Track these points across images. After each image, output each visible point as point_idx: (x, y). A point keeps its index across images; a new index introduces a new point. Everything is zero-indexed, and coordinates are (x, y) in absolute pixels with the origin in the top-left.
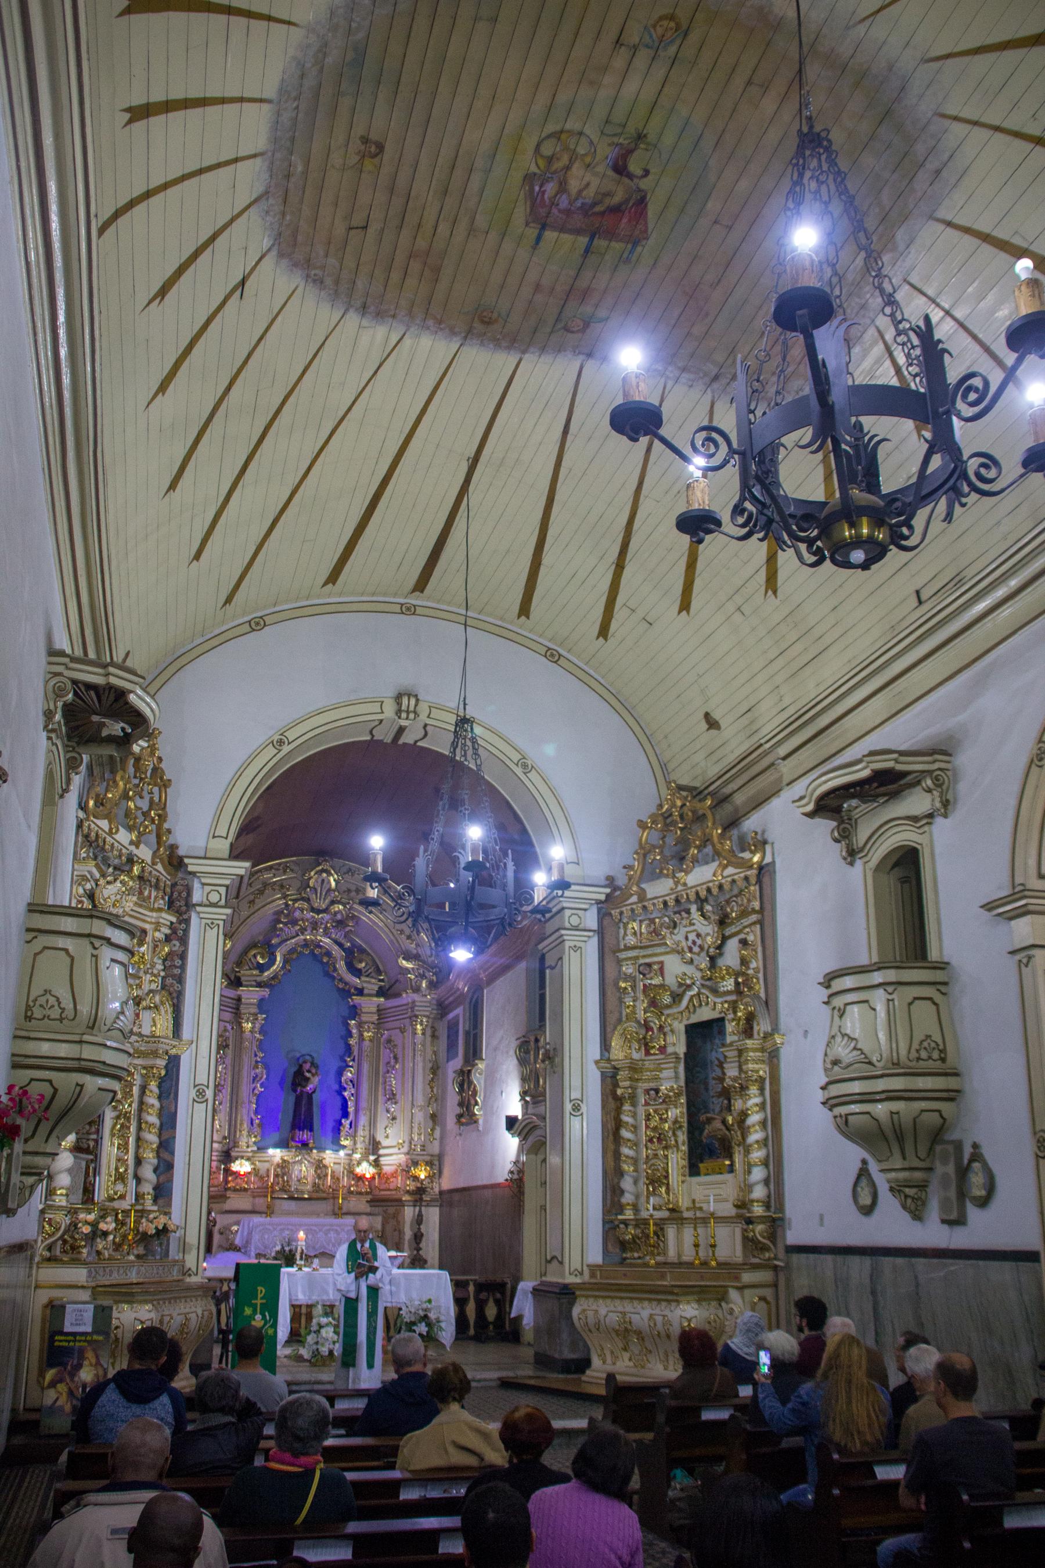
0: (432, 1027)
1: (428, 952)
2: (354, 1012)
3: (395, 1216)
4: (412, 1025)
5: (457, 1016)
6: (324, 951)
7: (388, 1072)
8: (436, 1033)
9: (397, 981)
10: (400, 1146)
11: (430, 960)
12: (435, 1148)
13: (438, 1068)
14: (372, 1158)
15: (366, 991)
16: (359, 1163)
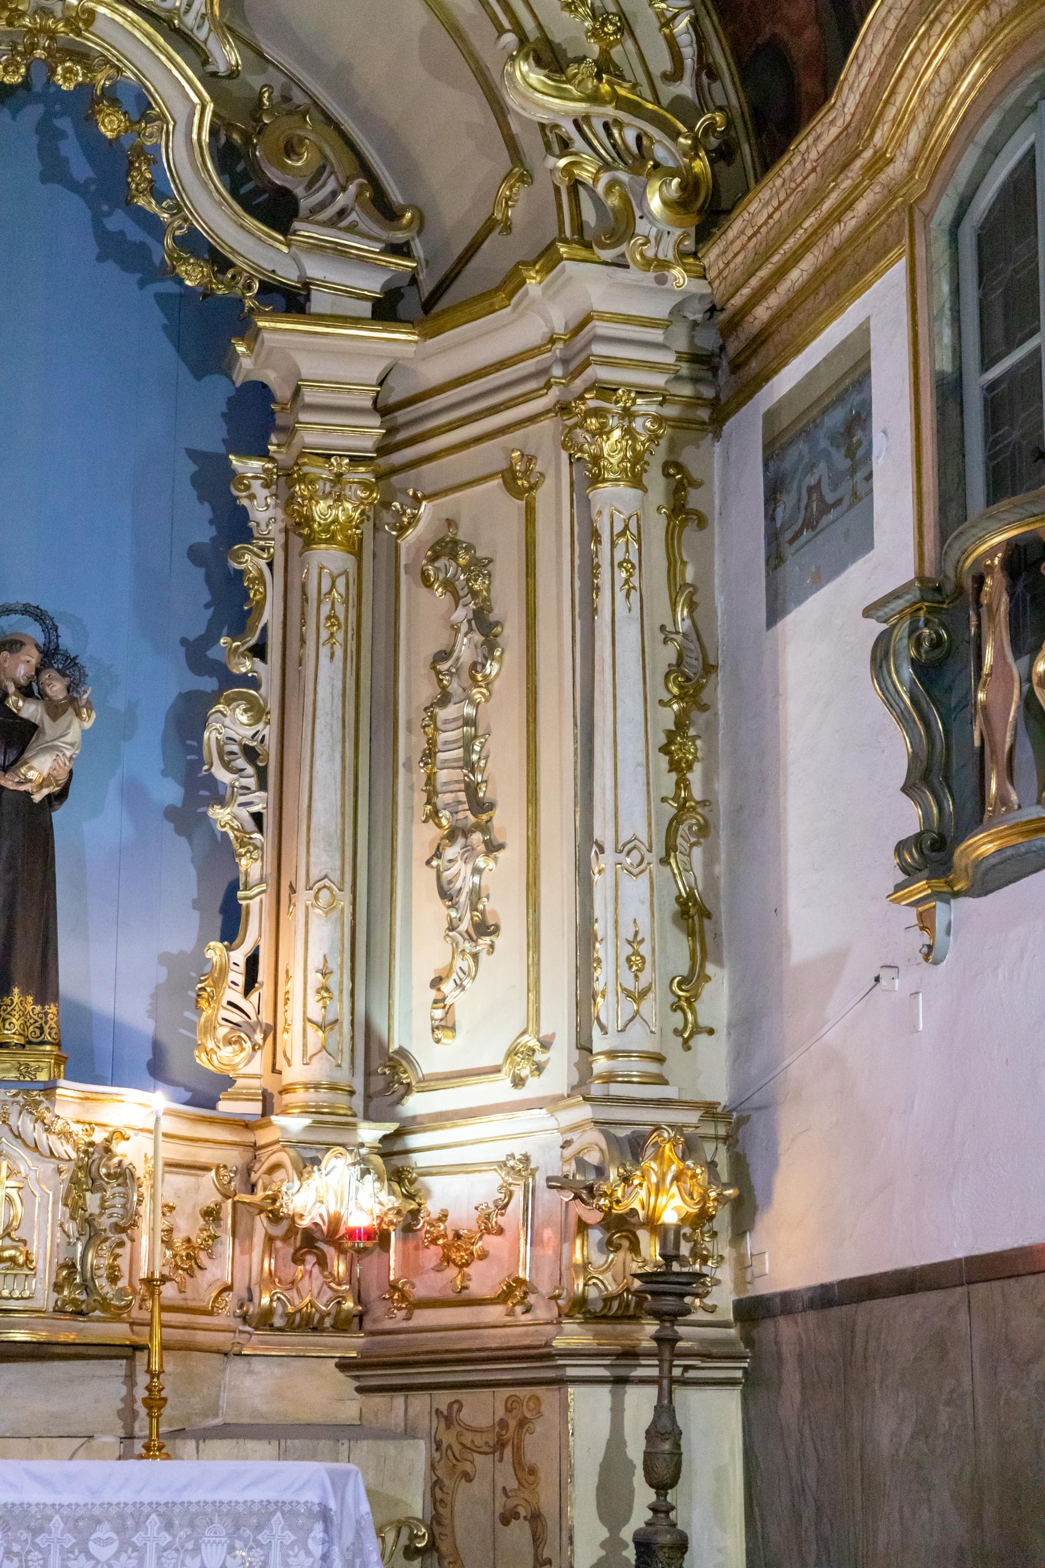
0: (672, 466)
1: (661, 62)
2: (257, 416)
3: (505, 1440)
4: (568, 443)
5: (864, 331)
6: (102, 80)
7: (444, 699)
8: (694, 499)
9: (489, 226)
10: (524, 1058)
11: (669, 91)
12: (709, 1073)
13: (709, 669)
14: (370, 1133)
15: (319, 302)
16: (308, 1162)
